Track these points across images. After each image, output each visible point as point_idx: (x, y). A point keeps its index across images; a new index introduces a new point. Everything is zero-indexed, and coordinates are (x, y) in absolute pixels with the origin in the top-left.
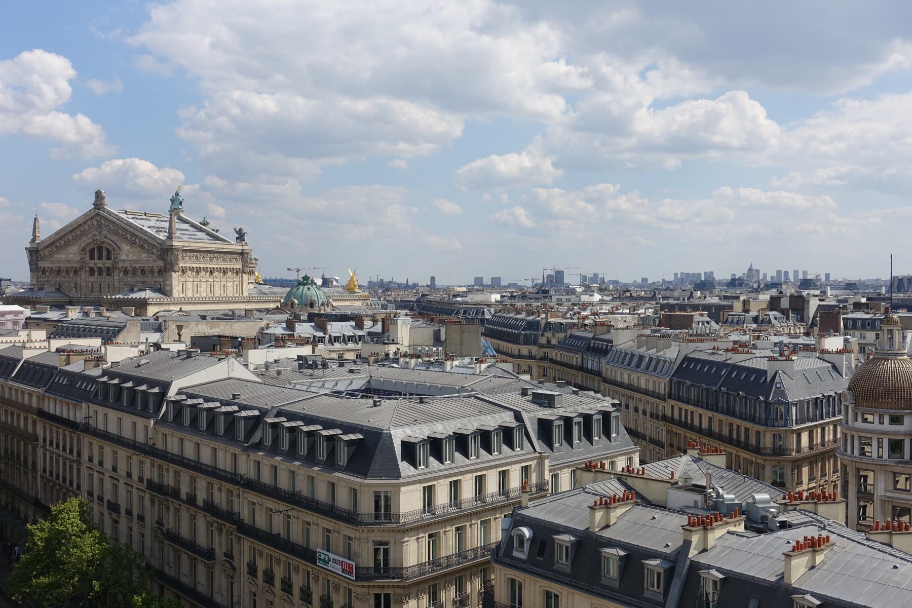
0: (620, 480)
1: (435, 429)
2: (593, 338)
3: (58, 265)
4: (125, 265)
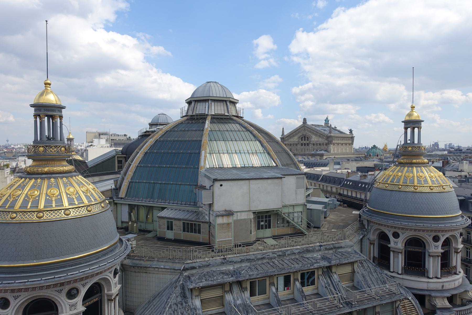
3: (290, 143)
4: (313, 142)
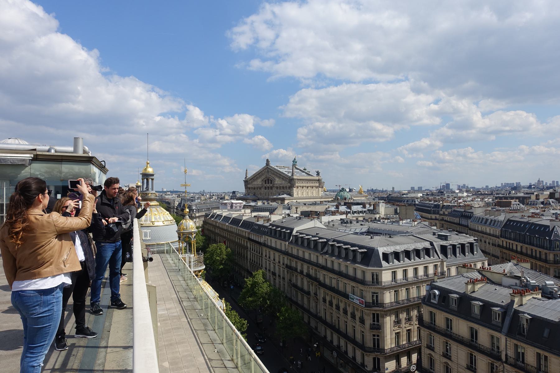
0: (479, 272)
1: (396, 248)
2: (464, 212)
4: (277, 185)
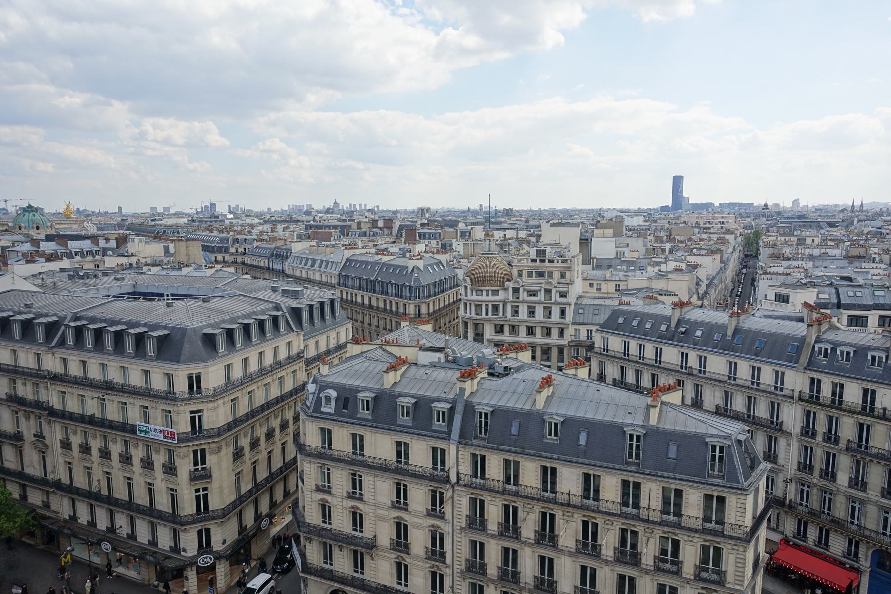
2: (275, 248)
